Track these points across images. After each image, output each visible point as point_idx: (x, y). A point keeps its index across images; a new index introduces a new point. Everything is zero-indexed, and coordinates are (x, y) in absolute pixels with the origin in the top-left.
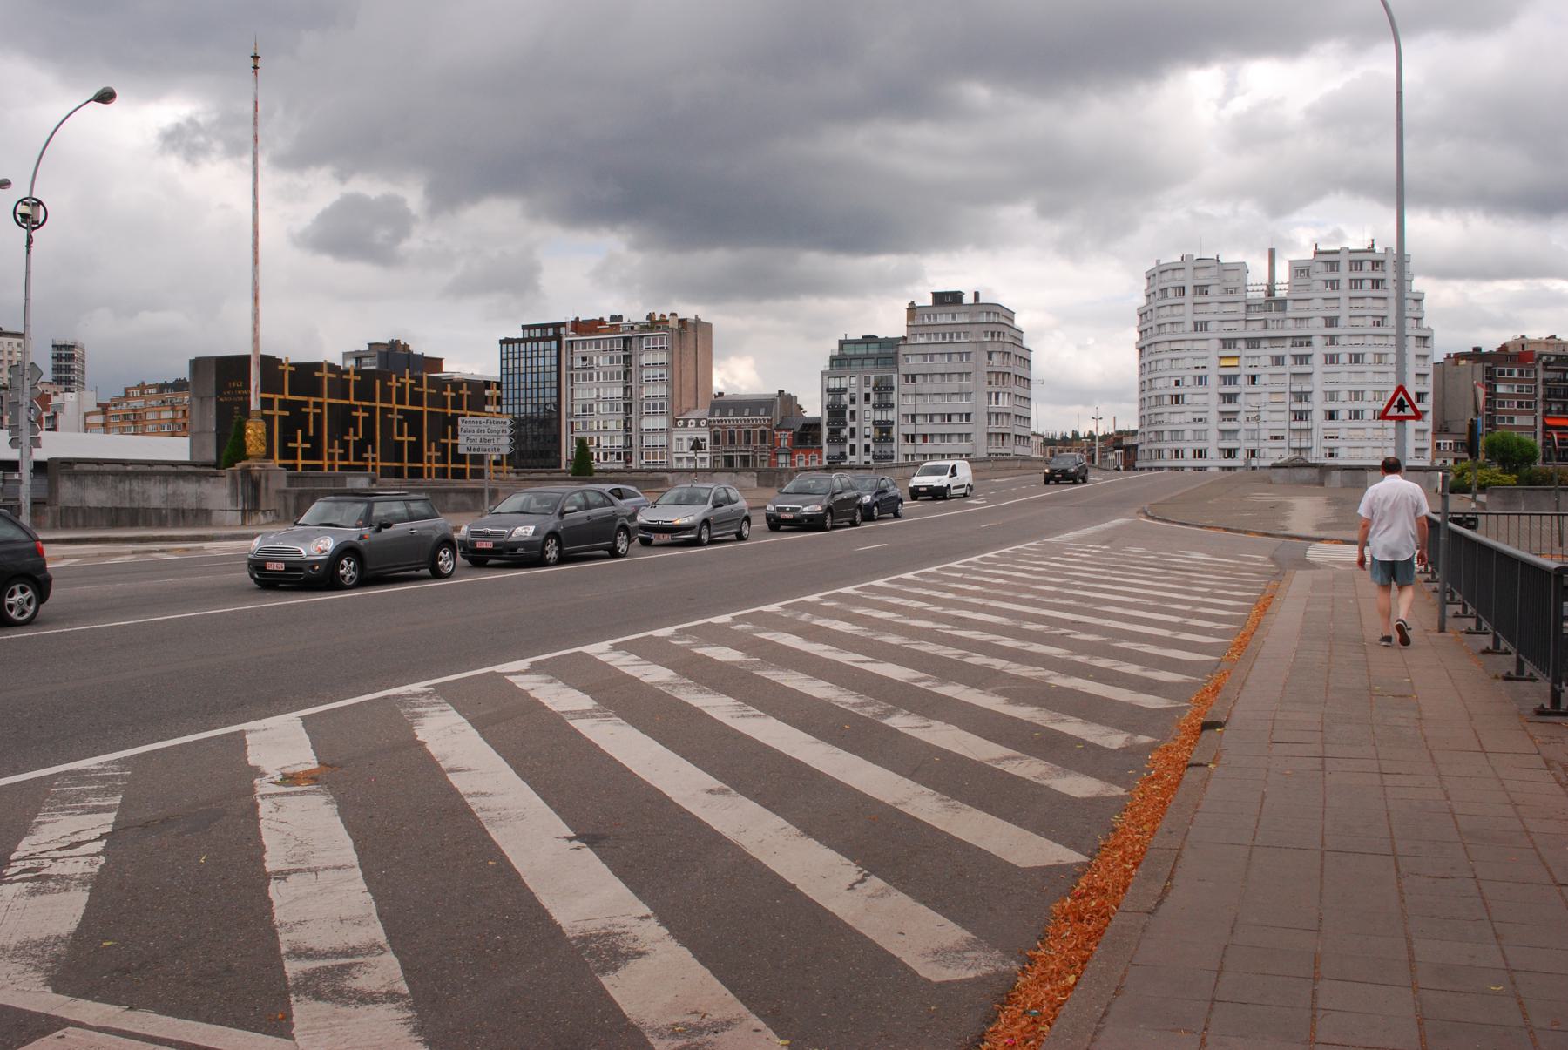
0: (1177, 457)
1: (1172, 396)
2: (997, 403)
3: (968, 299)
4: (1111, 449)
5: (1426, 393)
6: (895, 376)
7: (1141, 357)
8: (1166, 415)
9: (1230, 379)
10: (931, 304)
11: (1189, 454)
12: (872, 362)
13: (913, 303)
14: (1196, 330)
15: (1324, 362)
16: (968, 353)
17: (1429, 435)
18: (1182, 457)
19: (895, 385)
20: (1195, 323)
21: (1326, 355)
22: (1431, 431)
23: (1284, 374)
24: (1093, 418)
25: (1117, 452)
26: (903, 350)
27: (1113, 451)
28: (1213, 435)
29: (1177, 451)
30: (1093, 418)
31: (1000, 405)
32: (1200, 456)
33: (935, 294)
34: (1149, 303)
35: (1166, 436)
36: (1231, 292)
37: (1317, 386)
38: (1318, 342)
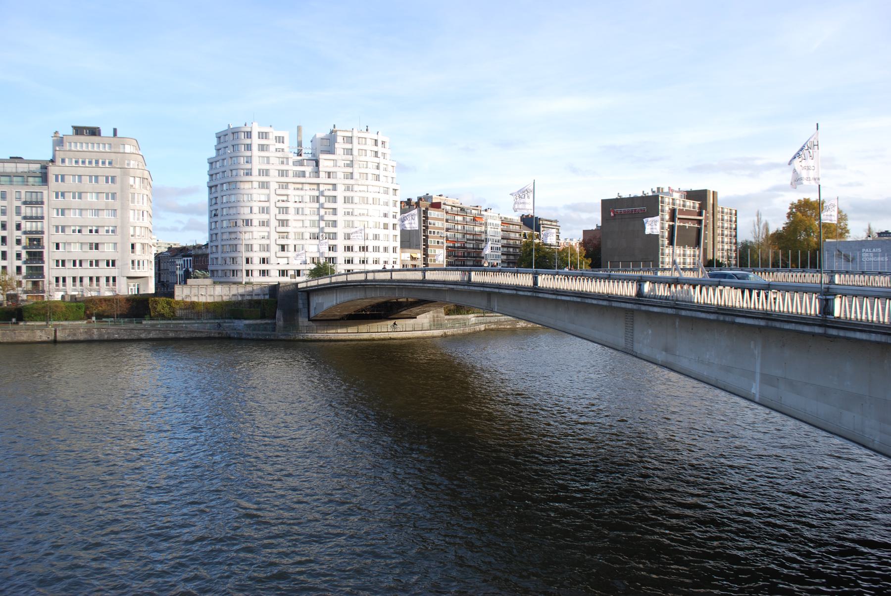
3: (106, 132)
6: (45, 193)
7: (210, 193)
9: (285, 210)
10: (71, 134)
12: (19, 179)
13: (56, 133)
14: (260, 175)
15: (343, 201)
16: (113, 178)
17: (398, 249)
19: (45, 200)
20: (259, 170)
21: (345, 197)
25: (186, 259)
26: (53, 170)
33: (74, 128)
34: (218, 155)
36: (279, 151)
37: (340, 218)
38: (341, 188)
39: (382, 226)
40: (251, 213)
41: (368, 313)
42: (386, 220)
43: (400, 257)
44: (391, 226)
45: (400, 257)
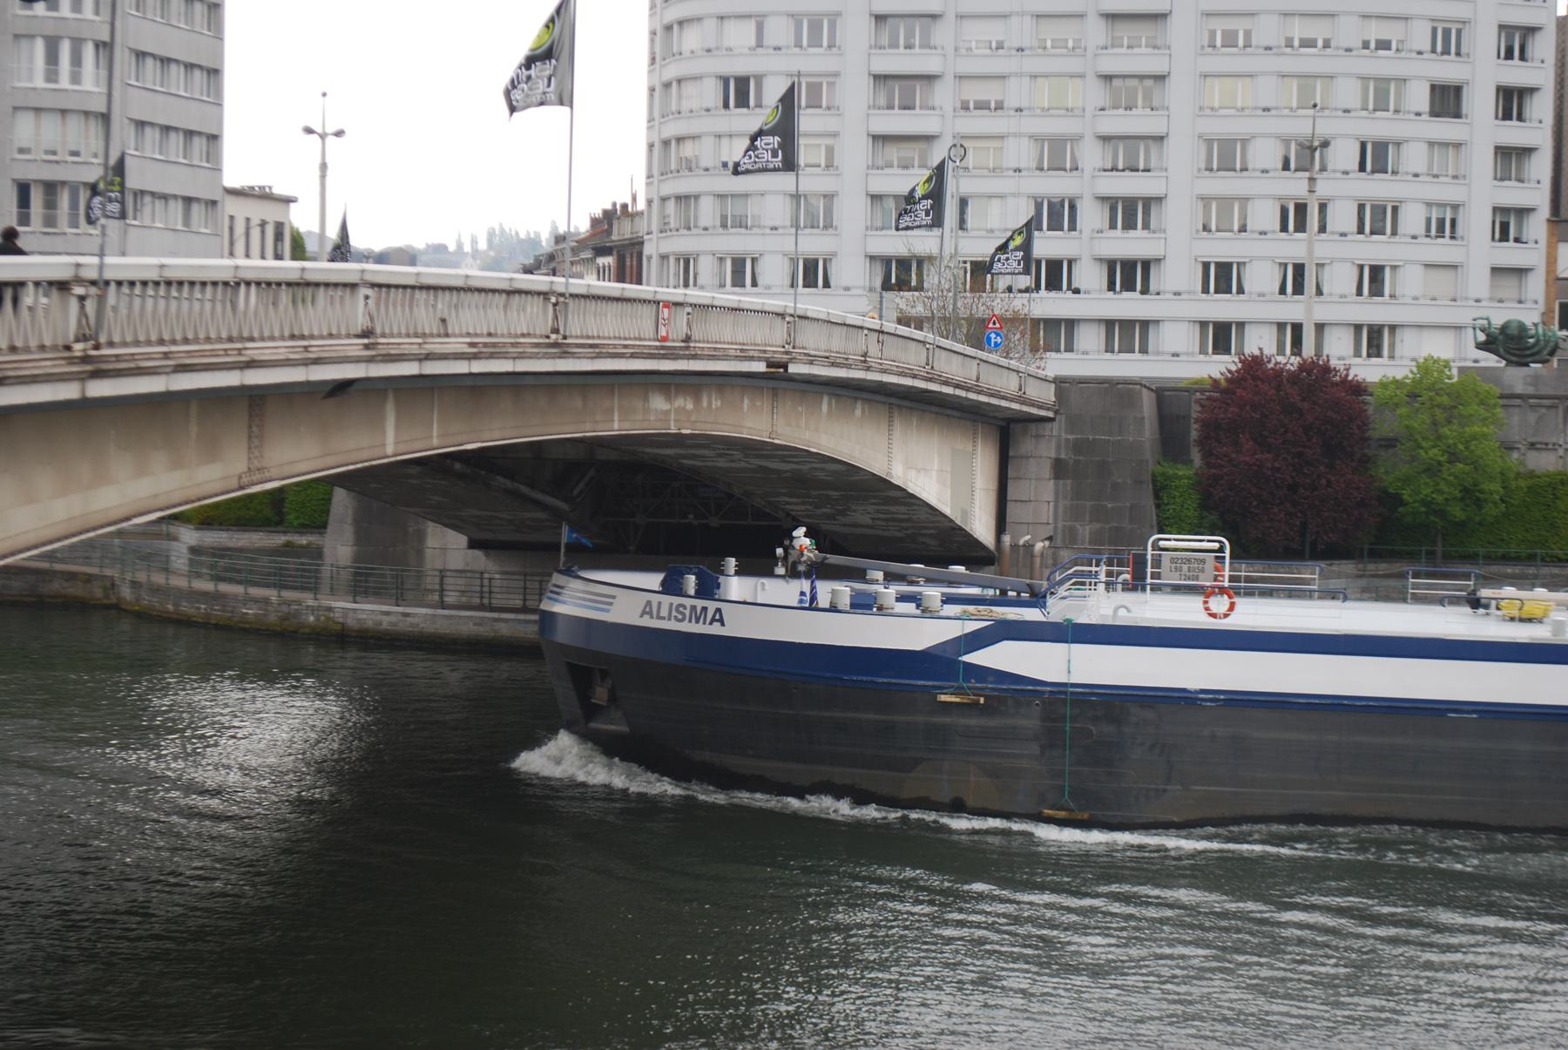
0: (738, 281)
1: (725, 81)
2: (76, 78)
4: (587, 254)
5: (1532, 90)
8: (708, 142)
11: (774, 271)
17: (1537, 227)
18: (754, 284)
22: (1544, 211)
23: (1081, 16)
24: (309, 131)
27: (593, 260)
28: (852, 212)
29: (738, 264)
30: (309, 131)
31: (64, 82)
32: (810, 282)
35: (707, 212)
39: (1419, 97)
40: (760, 44)
41: (715, 522)
42: (1448, 71)
43: (1552, 261)
44: (1481, 103)
45: (1552, 261)
